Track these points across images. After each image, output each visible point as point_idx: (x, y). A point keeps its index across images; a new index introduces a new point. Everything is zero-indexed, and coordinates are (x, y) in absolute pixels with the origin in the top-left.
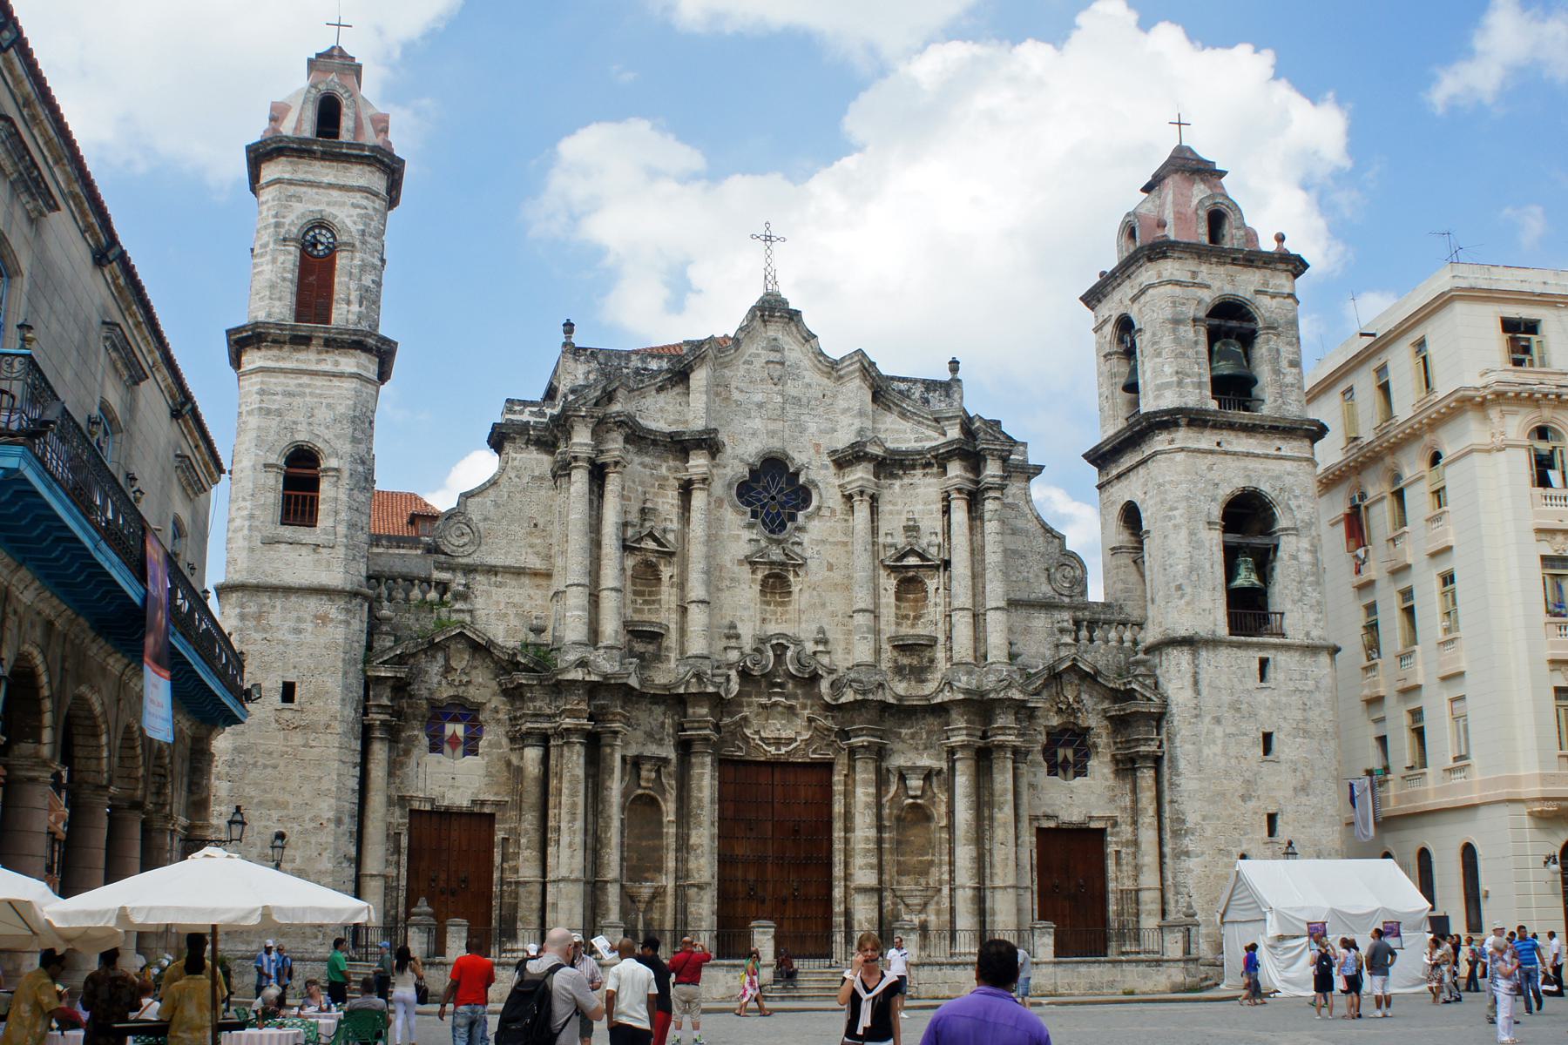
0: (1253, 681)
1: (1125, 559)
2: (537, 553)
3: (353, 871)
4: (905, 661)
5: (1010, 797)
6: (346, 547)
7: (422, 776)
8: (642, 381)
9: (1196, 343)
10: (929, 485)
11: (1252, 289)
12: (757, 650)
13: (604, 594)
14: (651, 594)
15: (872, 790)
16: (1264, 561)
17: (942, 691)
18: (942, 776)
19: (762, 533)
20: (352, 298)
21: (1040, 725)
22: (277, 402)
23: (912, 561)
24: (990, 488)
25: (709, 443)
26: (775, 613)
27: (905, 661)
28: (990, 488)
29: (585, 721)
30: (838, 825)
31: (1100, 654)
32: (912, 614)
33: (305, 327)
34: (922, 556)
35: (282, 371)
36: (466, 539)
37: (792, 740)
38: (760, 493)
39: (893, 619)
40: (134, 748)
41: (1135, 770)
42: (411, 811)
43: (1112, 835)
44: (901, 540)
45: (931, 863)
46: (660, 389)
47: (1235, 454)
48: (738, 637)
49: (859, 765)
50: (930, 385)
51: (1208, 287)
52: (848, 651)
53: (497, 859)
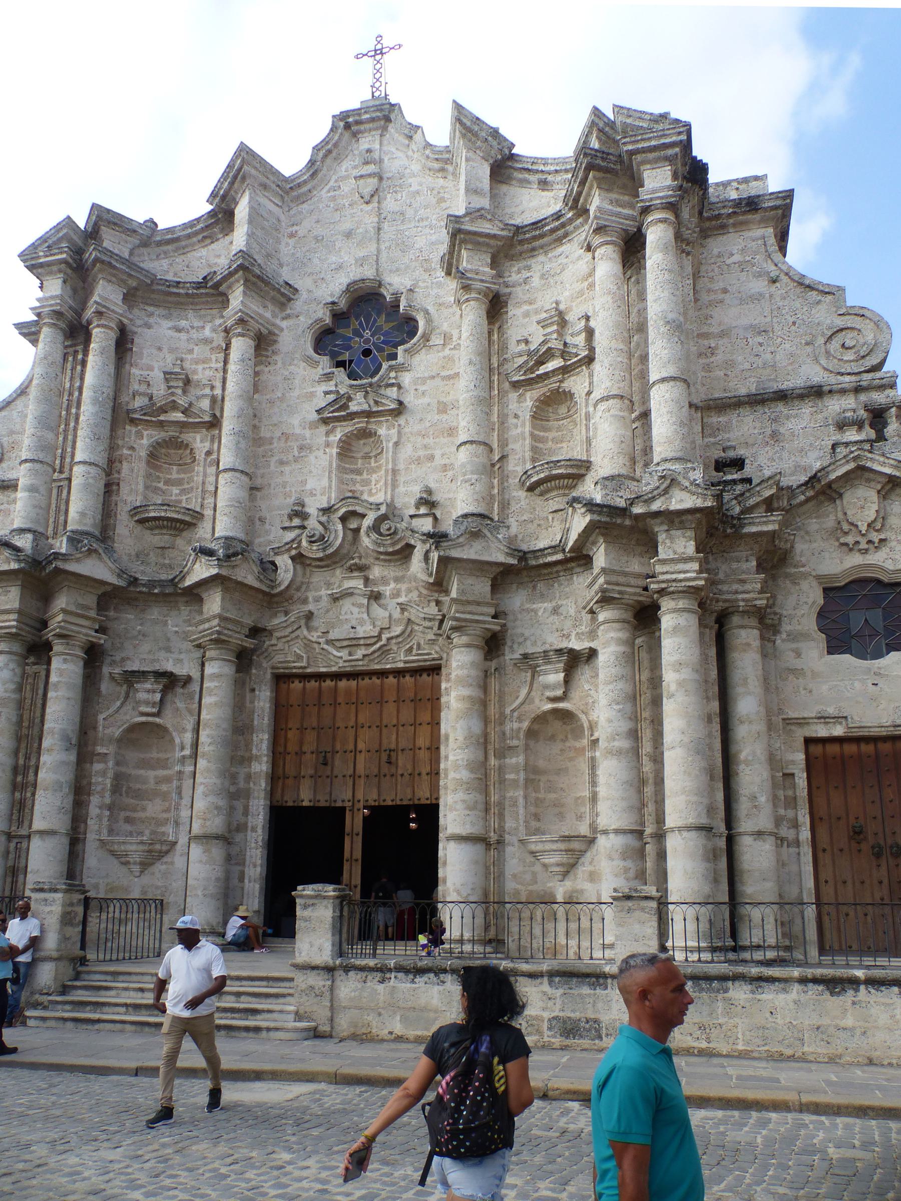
38: (350, 339)
48: (304, 516)
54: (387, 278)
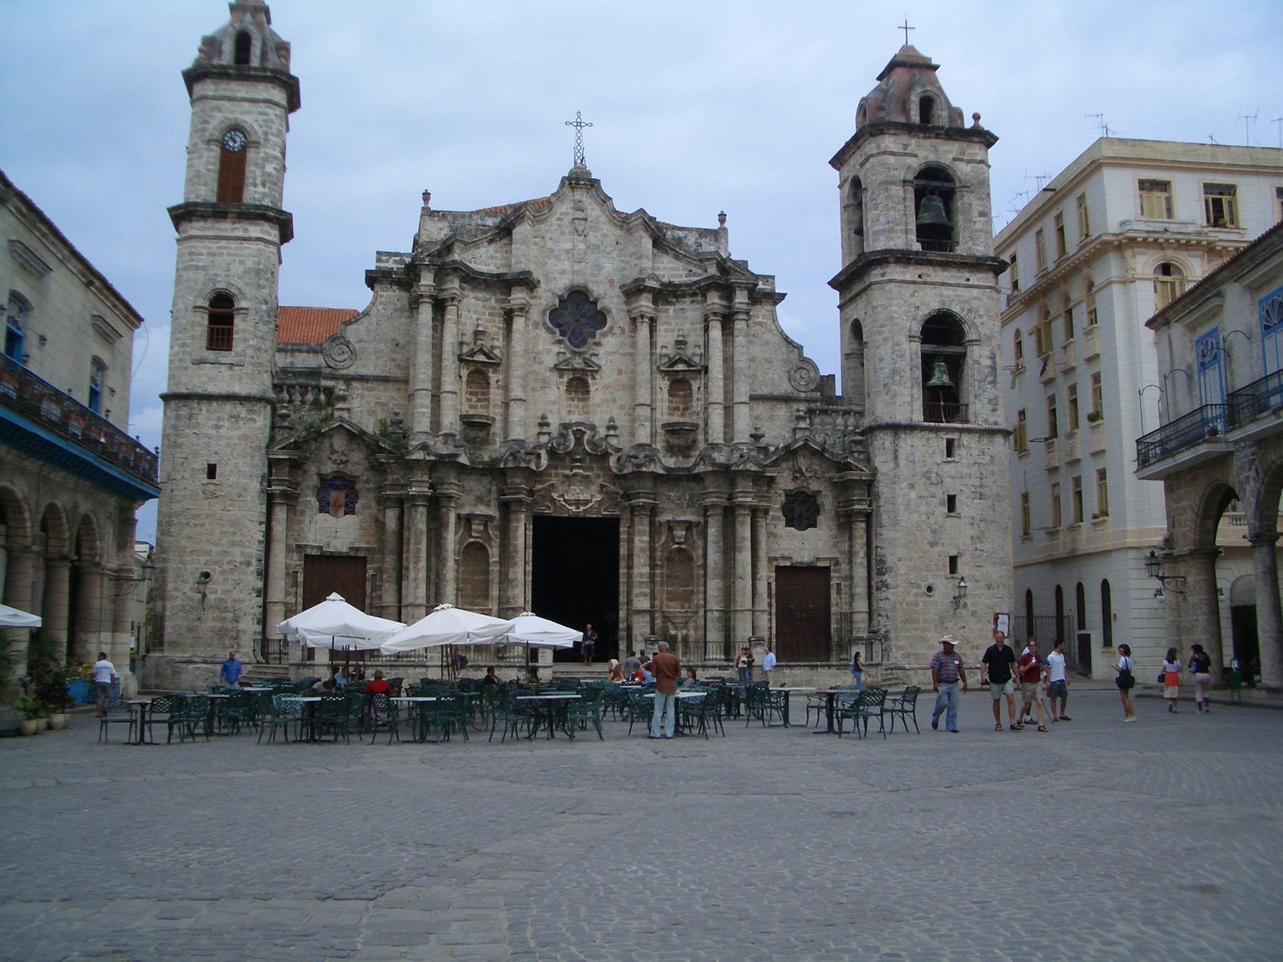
0: (941, 456)
1: (854, 363)
2: (398, 366)
3: (260, 600)
4: (675, 441)
5: (748, 544)
6: (253, 364)
7: (313, 530)
8: (476, 236)
9: (905, 199)
10: (695, 310)
11: (951, 157)
12: (562, 435)
13: (443, 395)
14: (483, 394)
15: (648, 539)
16: (956, 365)
17: (698, 464)
18: (701, 528)
19: (566, 347)
20: (259, 182)
21: (780, 489)
22: (203, 261)
23: (681, 367)
24: (738, 312)
25: (526, 281)
26: (577, 407)
27: (675, 441)
28: (738, 312)
29: (427, 490)
30: (623, 564)
31: (828, 433)
32: (682, 407)
33: (222, 207)
34: (688, 363)
35: (206, 237)
36: (345, 356)
37: (587, 502)
39: (665, 410)
40: (60, 519)
41: (851, 523)
42: (307, 557)
43: (835, 571)
44: (671, 351)
45: (692, 592)
46: (491, 242)
47: (933, 284)
48: (548, 425)
49: (637, 519)
50: (703, 233)
51: (916, 156)
52: (632, 434)
53: (368, 589)
54: (591, 286)
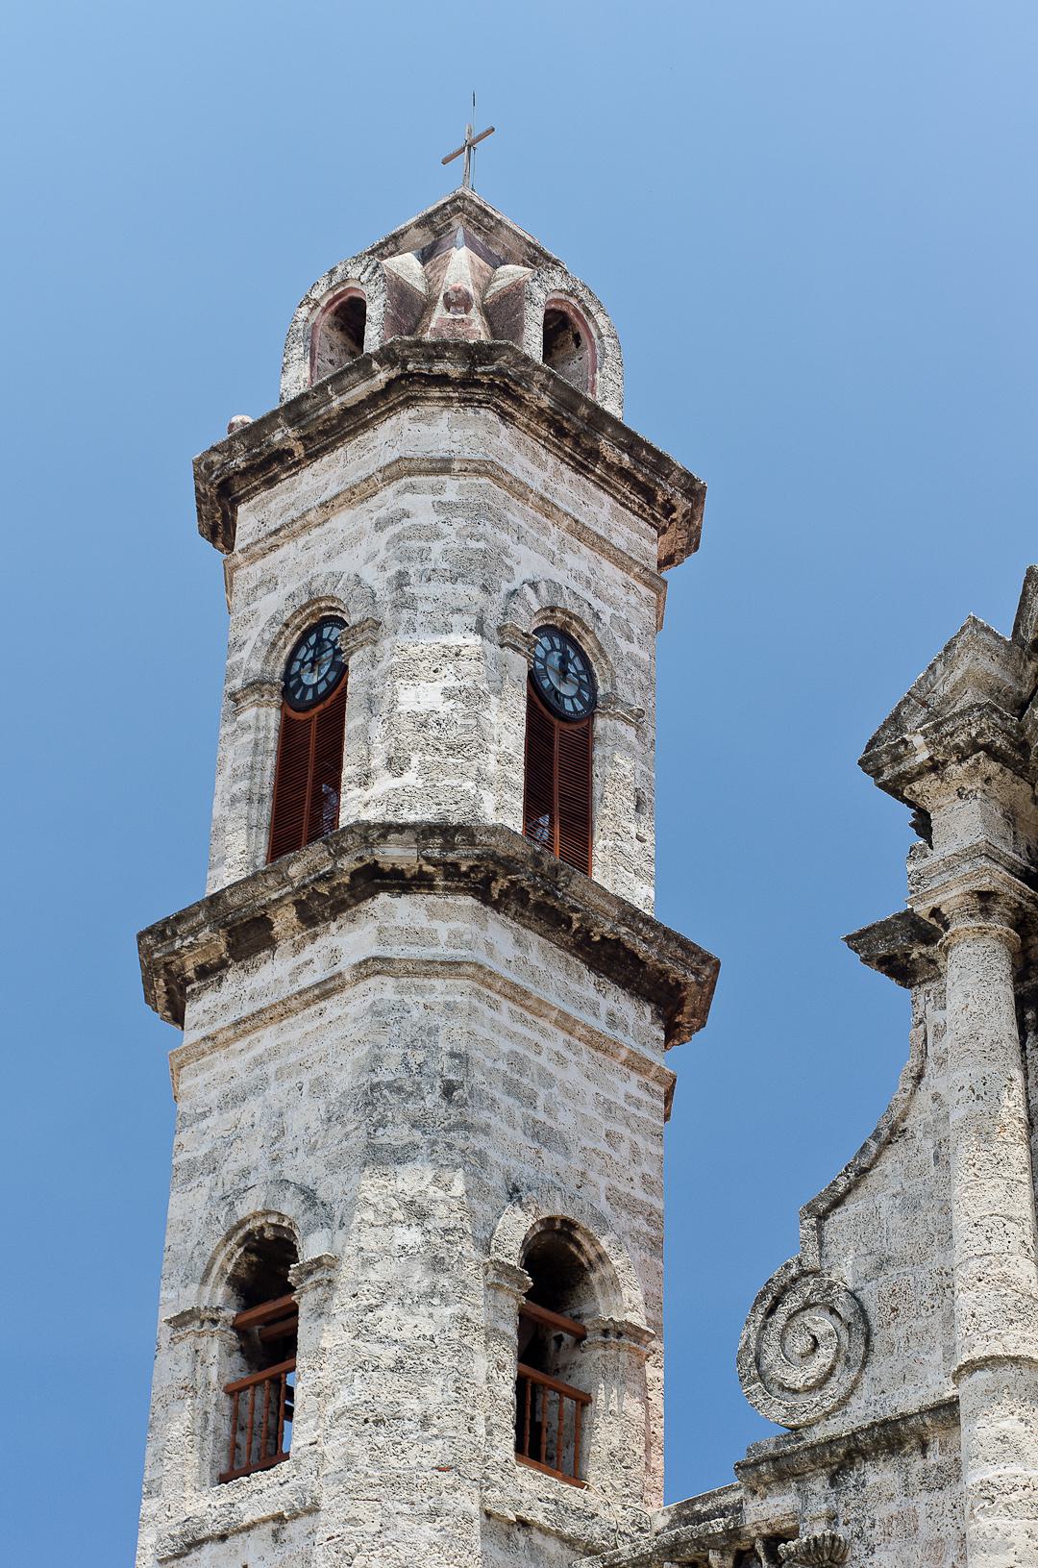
36: (824, 1358)
